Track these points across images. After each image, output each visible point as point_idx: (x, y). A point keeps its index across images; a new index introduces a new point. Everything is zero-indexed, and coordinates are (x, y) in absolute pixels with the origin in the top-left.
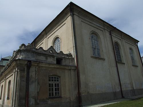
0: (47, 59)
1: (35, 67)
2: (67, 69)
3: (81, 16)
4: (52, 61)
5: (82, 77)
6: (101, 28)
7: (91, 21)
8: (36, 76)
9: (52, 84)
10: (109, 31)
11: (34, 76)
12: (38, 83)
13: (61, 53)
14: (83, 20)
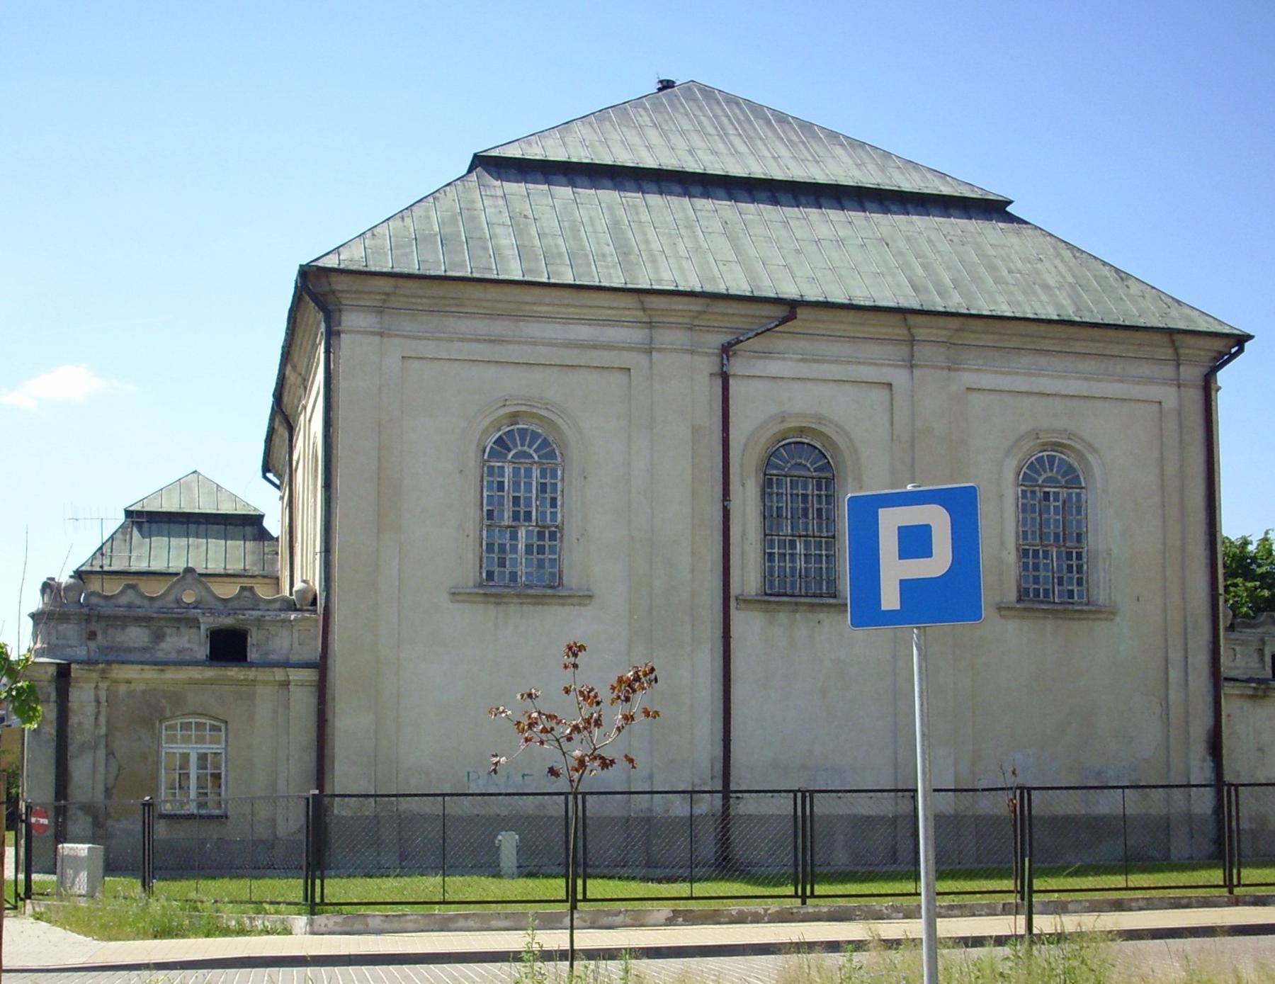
0: (159, 637)
1: (93, 685)
2: (265, 683)
3: (406, 325)
4: (187, 646)
5: (348, 723)
6: (610, 347)
7: (499, 328)
8: (97, 725)
9: (185, 757)
11: (88, 722)
12: (110, 754)
13: (246, 593)
14: (427, 348)
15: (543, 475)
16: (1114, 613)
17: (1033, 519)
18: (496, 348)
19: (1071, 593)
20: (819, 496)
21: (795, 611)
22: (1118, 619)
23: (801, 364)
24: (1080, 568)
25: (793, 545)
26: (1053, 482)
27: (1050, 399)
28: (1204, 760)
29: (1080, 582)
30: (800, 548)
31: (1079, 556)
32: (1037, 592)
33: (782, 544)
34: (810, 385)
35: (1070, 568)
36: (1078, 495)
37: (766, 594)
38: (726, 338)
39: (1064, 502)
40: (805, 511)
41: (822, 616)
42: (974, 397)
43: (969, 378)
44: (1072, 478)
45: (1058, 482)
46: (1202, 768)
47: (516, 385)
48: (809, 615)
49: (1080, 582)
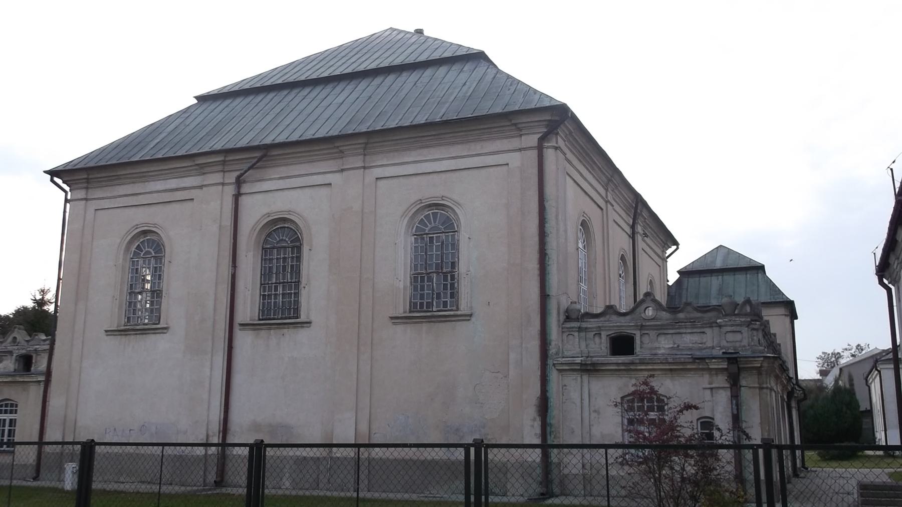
3: (98, 193)
5: (56, 402)
10: (232, 177)
14: (106, 204)
15: (156, 263)
16: (471, 315)
17: (422, 256)
18: (135, 198)
19: (445, 303)
20: (293, 258)
21: (270, 329)
22: (473, 319)
23: (281, 181)
24: (452, 285)
25: (276, 290)
26: (435, 229)
27: (431, 176)
28: (534, 420)
29: (452, 296)
30: (280, 290)
31: (453, 278)
32: (422, 304)
33: (270, 289)
34: (286, 192)
35: (445, 286)
36: (453, 236)
37: (260, 320)
38: (238, 173)
39: (443, 243)
40: (284, 267)
41: (285, 331)
42: (381, 183)
43: (378, 172)
44: (450, 226)
45: (440, 229)
46: (532, 426)
47: (141, 217)
48: (277, 331)
49: (452, 296)
